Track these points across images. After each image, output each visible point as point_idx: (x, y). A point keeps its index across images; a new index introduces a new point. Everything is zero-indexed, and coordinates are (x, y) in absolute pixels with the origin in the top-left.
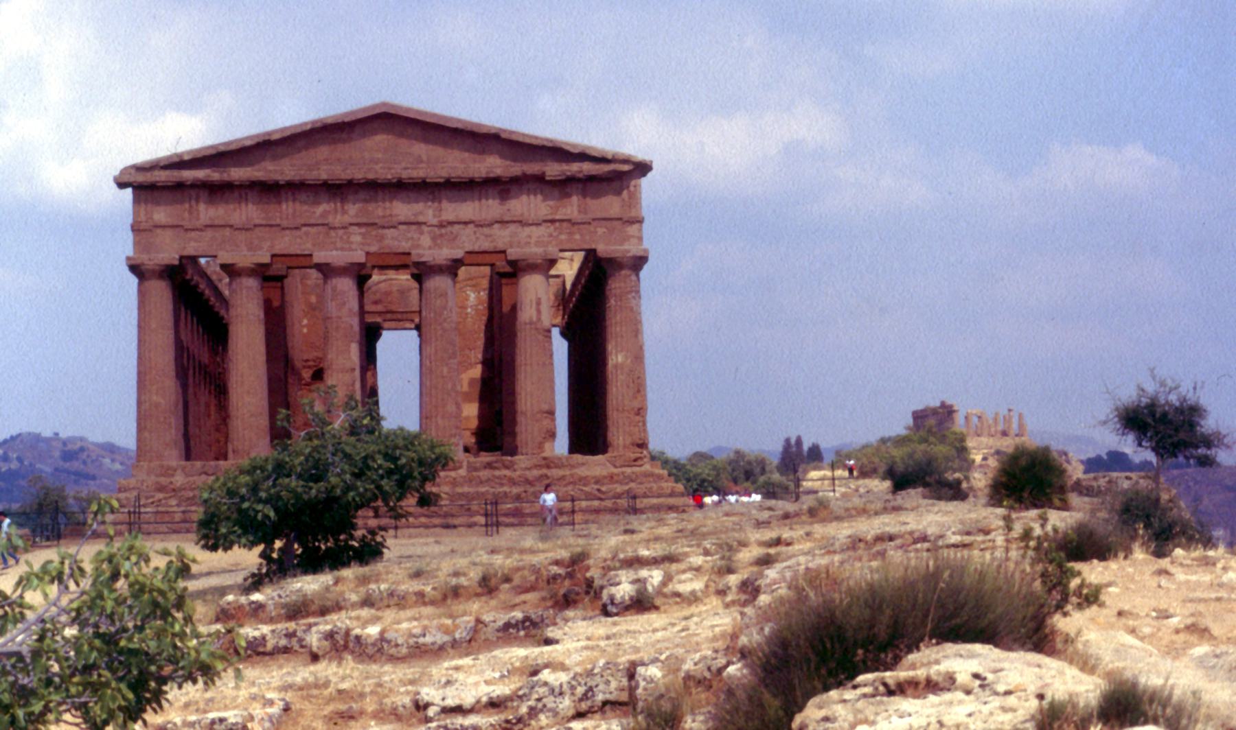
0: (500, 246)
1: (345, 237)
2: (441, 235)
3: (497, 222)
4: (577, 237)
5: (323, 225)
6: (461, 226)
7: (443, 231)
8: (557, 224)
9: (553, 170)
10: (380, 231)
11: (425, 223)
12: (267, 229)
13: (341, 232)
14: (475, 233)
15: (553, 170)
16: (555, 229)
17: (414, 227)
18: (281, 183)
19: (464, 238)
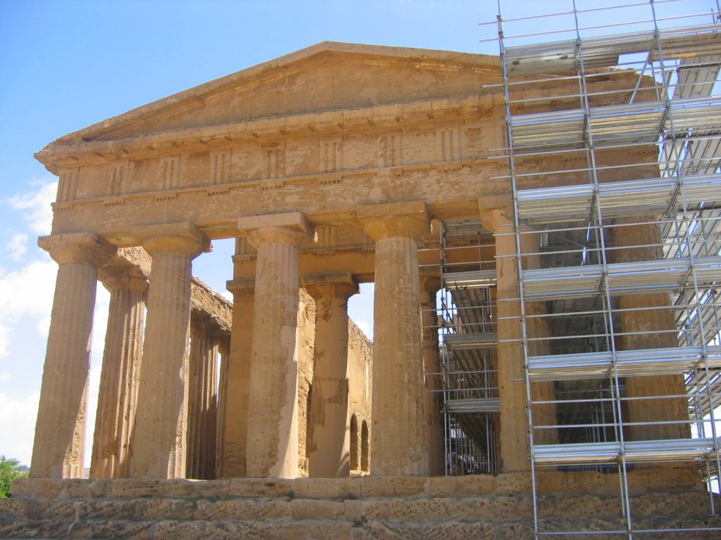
6: (420, 175)
7: (398, 182)
10: (322, 188)
13: (274, 192)
14: (438, 181)
17: (361, 180)
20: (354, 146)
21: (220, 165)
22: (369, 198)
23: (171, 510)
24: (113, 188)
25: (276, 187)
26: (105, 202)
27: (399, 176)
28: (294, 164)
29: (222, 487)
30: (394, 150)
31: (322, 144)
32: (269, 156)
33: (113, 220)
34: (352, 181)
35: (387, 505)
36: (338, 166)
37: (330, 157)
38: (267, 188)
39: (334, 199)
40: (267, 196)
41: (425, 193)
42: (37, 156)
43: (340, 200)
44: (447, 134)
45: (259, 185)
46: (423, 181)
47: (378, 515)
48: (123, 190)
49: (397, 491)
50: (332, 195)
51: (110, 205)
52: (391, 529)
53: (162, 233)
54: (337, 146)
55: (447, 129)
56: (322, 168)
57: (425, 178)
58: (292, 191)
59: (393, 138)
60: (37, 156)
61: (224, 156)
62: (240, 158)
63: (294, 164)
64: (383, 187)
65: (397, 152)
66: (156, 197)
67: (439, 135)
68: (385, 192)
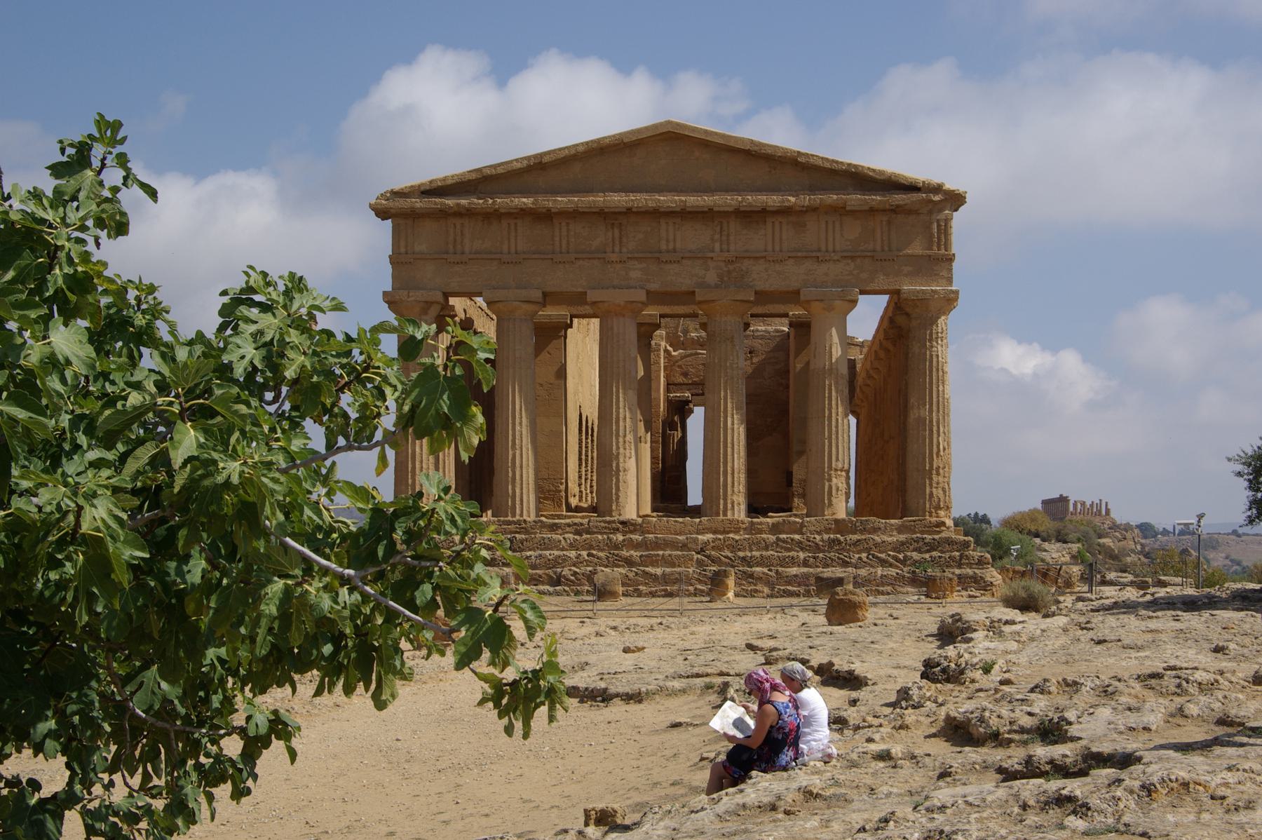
2: (729, 272)
7: (731, 267)
8: (859, 260)
11: (712, 258)
18: (553, 210)
21: (564, 233)
23: (545, 543)
24: (454, 247)
29: (582, 524)
30: (728, 235)
31: (663, 221)
32: (613, 228)
35: (720, 539)
36: (678, 245)
37: (671, 237)
41: (754, 280)
42: (371, 205)
44: (777, 225)
45: (604, 258)
47: (713, 547)
48: (467, 250)
49: (727, 529)
52: (725, 557)
54: (677, 226)
56: (664, 247)
57: (755, 265)
59: (728, 223)
60: (373, 208)
61: (568, 224)
62: (584, 227)
65: (732, 238)
67: (769, 226)
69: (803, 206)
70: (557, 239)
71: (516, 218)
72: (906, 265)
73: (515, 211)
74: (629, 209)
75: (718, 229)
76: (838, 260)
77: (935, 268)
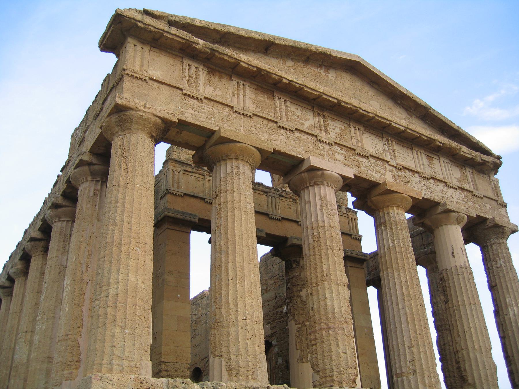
0: (437, 199)
1: (331, 153)
2: (399, 176)
3: (432, 177)
4: (477, 206)
5: (312, 135)
6: (410, 173)
7: (400, 174)
8: (465, 193)
9: (465, 150)
10: (357, 157)
11: (388, 162)
12: (265, 122)
13: (327, 147)
15: (465, 150)
16: (465, 196)
17: (380, 163)
18: (284, 80)
19: (414, 183)
20: (370, 137)
22: (386, 177)
25: (329, 143)
26: (184, 92)
27: (401, 169)
28: (335, 131)
30: (394, 151)
33: (193, 112)
34: (374, 161)
38: (323, 141)
39: (366, 169)
40: (321, 148)
43: (369, 172)
46: (412, 178)
50: (364, 165)
51: (189, 96)
53: (249, 143)
55: (419, 151)
58: (338, 151)
62: (297, 109)
63: (335, 131)
64: (392, 173)
66: (235, 109)
68: (394, 177)
69: (441, 143)
70: (278, 109)
71: (244, 81)
72: (487, 203)
73: (255, 69)
74: (339, 101)
75: (386, 143)
76: (456, 189)
77: (501, 210)
